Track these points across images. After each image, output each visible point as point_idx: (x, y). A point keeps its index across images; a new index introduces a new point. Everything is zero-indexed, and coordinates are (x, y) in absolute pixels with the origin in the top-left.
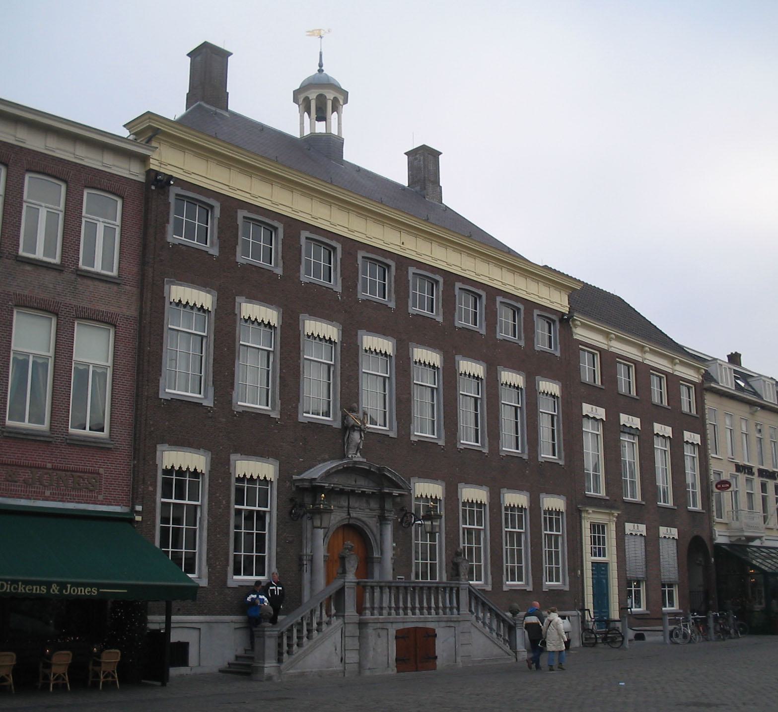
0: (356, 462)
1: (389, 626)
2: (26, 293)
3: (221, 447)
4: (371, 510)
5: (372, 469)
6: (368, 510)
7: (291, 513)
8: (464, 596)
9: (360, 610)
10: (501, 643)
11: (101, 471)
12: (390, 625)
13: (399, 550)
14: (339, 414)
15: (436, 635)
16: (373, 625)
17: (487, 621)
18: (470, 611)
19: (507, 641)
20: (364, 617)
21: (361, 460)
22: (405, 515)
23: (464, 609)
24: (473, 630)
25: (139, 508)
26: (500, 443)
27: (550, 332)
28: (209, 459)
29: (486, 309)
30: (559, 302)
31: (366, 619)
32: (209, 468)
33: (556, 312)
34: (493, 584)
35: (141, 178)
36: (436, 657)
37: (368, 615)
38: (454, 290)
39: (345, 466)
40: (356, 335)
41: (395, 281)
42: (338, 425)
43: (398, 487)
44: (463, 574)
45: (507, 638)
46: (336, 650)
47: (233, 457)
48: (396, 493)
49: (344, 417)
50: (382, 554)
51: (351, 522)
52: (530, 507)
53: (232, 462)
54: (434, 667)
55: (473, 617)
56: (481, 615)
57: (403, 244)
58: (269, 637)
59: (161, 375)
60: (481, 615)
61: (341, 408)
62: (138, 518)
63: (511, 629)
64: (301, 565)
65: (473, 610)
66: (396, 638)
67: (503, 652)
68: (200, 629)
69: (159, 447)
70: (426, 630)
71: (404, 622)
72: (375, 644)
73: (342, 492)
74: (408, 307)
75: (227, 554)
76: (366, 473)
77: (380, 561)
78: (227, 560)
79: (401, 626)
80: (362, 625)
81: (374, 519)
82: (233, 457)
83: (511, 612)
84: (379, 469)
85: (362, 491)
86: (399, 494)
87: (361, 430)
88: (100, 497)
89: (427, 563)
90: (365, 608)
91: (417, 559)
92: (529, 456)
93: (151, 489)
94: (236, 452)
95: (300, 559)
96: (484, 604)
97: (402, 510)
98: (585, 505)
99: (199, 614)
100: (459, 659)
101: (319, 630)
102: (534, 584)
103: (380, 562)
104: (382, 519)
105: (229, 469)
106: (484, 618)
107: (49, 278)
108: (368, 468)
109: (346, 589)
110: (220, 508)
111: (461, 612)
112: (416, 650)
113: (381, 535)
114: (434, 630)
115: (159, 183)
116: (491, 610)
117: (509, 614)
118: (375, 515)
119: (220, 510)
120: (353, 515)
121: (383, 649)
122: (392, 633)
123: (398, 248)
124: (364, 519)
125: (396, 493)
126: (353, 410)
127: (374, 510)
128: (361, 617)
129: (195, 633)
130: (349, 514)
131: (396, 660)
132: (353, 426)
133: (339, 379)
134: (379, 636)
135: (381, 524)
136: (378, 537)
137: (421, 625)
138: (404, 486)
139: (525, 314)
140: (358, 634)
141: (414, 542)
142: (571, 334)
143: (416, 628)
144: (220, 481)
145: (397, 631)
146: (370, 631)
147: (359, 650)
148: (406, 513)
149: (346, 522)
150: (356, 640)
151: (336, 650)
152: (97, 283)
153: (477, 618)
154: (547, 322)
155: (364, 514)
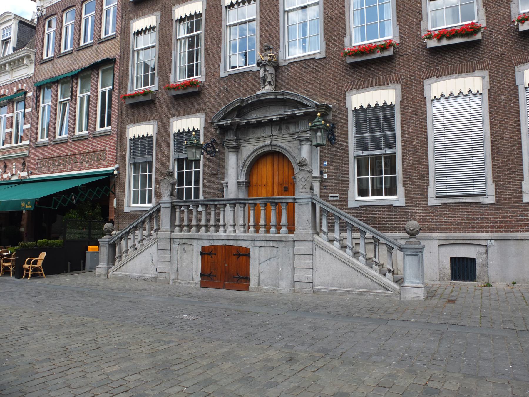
0: (258, 96)
4: (290, 134)
5: (278, 97)
6: (287, 136)
11: (107, 148)
12: (195, 241)
13: (332, 167)
15: (248, 255)
16: (178, 240)
32: (156, 132)
39: (250, 101)
48: (299, 112)
53: (170, 124)
66: (201, 254)
67: (376, 285)
70: (238, 248)
71: (210, 239)
79: (207, 243)
85: (269, 120)
86: (304, 112)
89: (382, 177)
93: (124, 153)
108: (274, 97)
112: (226, 268)
114: (247, 250)
122: (198, 247)
125: (299, 112)
131: (201, 275)
134: (184, 250)
137: (231, 243)
138: (308, 104)
145: (203, 248)
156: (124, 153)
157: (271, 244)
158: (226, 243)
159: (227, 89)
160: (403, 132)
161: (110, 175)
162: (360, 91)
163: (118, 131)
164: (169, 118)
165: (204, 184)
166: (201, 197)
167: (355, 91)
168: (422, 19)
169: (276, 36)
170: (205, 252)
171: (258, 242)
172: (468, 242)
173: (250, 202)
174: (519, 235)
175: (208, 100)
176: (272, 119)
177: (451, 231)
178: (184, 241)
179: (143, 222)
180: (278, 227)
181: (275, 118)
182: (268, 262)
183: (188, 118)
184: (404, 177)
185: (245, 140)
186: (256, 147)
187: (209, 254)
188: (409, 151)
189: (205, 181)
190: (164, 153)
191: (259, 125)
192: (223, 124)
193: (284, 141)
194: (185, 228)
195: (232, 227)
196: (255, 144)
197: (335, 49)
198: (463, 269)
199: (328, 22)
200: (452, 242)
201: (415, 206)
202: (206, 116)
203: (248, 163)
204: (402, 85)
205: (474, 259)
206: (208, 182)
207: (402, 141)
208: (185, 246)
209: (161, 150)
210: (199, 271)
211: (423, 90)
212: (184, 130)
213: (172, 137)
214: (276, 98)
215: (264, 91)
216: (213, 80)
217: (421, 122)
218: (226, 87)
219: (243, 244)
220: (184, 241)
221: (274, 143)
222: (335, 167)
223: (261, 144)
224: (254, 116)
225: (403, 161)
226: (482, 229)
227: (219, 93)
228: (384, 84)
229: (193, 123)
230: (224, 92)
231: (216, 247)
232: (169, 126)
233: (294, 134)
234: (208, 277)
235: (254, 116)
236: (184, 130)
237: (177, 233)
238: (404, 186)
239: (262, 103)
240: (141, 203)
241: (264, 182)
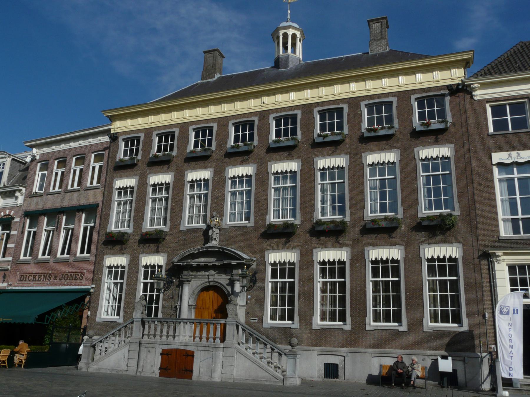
2: (67, 204)
11: (85, 271)
28: (129, 259)
32: (128, 263)
34: (353, 324)
36: (192, 371)
40: (225, 171)
48: (234, 262)
51: (211, 284)
53: (140, 258)
54: (190, 377)
57: (264, 103)
62: (92, 290)
66: (161, 354)
79: (166, 347)
88: (84, 283)
92: (461, 211)
93: (100, 276)
98: (500, 248)
107: (75, 194)
114: (193, 352)
125: (234, 262)
131: (160, 369)
134: (149, 351)
137: (182, 348)
145: (163, 350)
146: (142, 348)
149: (208, 284)
152: (91, 191)
156: (100, 276)
158: (180, 347)
159: (185, 239)
160: (300, 280)
161: (87, 292)
162: (274, 251)
163: (95, 260)
164: (139, 254)
165: (163, 305)
166: (160, 315)
167: (271, 251)
168: (314, 211)
169: (221, 208)
170: (164, 353)
172: (334, 353)
173: (197, 321)
174: (363, 350)
177: (325, 346)
178: (149, 345)
179: (119, 330)
184: (299, 310)
185: (195, 276)
186: (203, 282)
187: (167, 354)
188: (302, 293)
190: (133, 279)
195: (184, 337)
197: (260, 222)
198: (331, 371)
199: (257, 203)
200: (325, 353)
201: (305, 329)
202: (168, 256)
203: (196, 292)
205: (337, 365)
206: (165, 304)
207: (299, 286)
208: (150, 348)
209: (131, 277)
210: (159, 366)
214: (218, 251)
215: (211, 245)
217: (311, 275)
218: (184, 237)
221: (216, 280)
222: (256, 300)
223: (207, 280)
224: (202, 260)
225: (299, 299)
226: (342, 346)
227: (179, 241)
229: (158, 260)
230: (182, 240)
232: (139, 260)
238: (299, 315)
241: (207, 306)
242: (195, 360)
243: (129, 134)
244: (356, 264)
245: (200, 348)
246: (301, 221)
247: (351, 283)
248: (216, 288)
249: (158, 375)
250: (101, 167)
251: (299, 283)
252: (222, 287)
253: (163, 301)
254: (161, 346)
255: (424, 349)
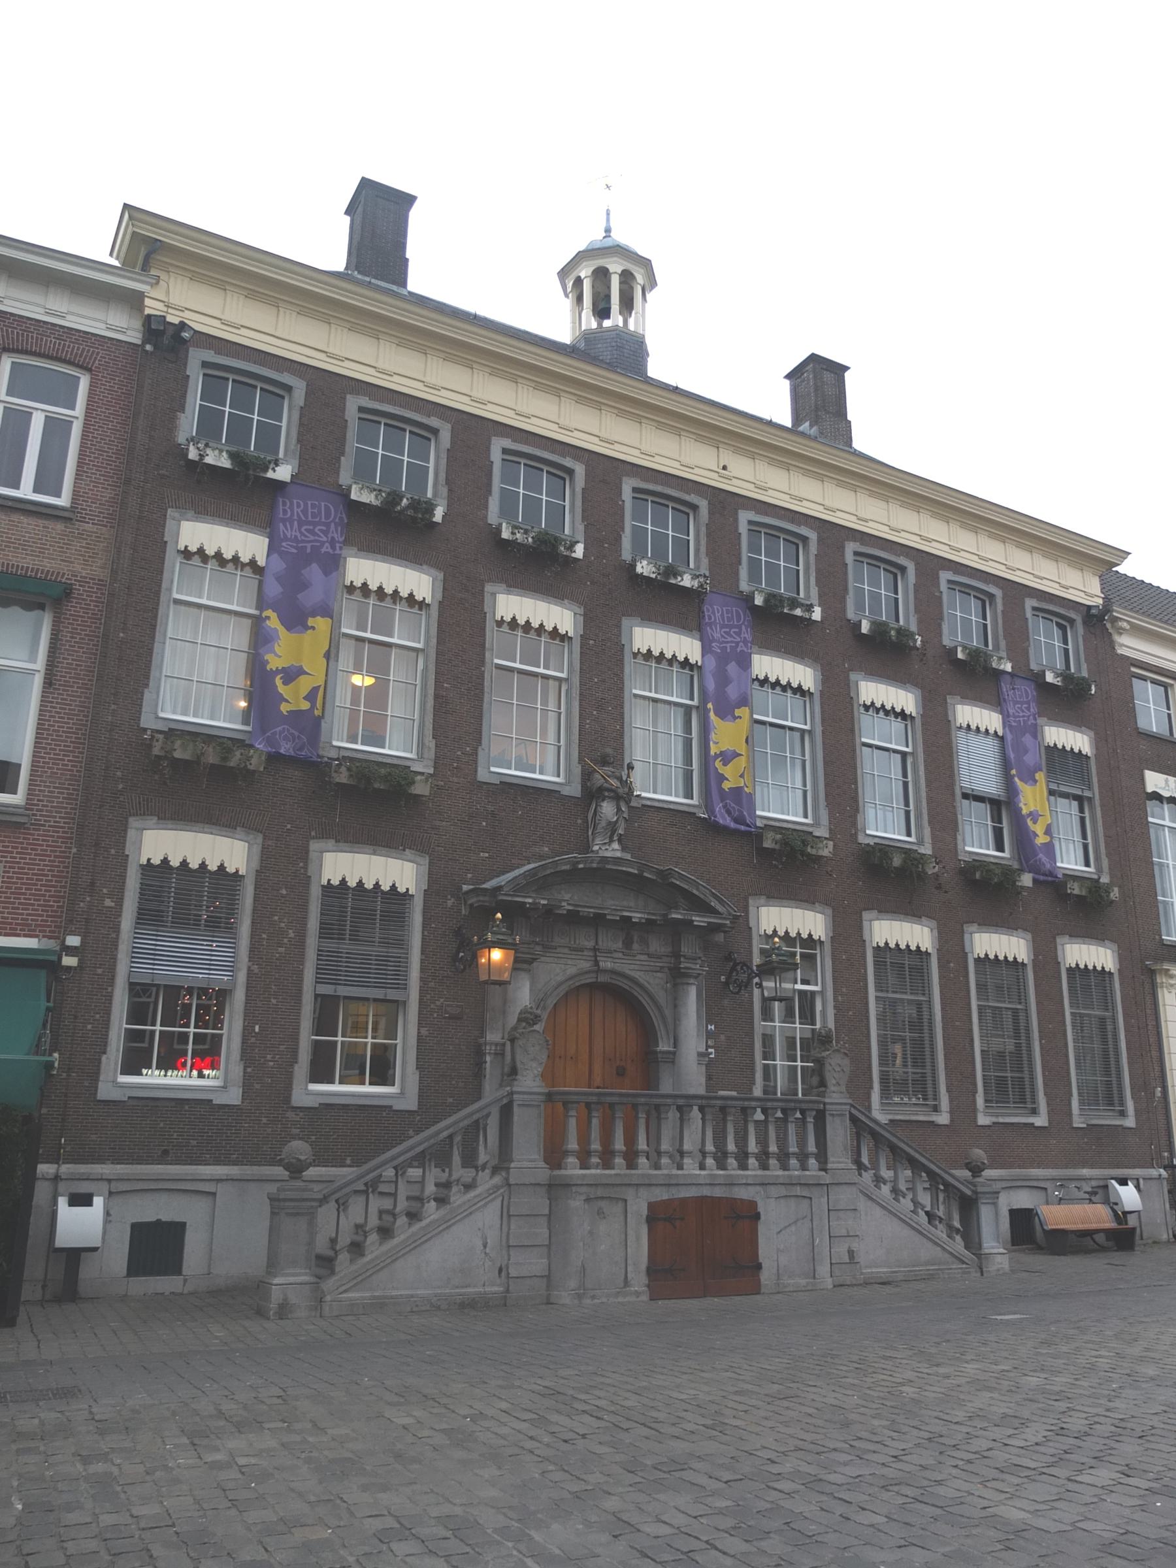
0: (604, 859)
1: (629, 1194)
3: (289, 826)
5: (646, 874)
7: (455, 958)
8: (838, 1133)
9: (554, 1155)
10: (941, 1233)
13: (722, 1037)
14: (577, 770)
15: (757, 1216)
16: (584, 1189)
17: (902, 1186)
18: (860, 1166)
19: (958, 1231)
20: (563, 1172)
21: (618, 854)
22: (733, 969)
23: (840, 1159)
24: (862, 1204)
25: (73, 941)
26: (959, 837)
27: (1065, 642)
28: (257, 849)
29: (916, 591)
30: (1085, 589)
31: (571, 1176)
33: (1075, 605)
34: (951, 1112)
35: (134, 336)
36: (759, 1267)
37: (572, 1170)
38: (843, 555)
39: (581, 866)
41: (708, 535)
42: (575, 790)
43: (703, 907)
44: (834, 1082)
45: (957, 1224)
46: (485, 1246)
47: (314, 846)
48: (699, 920)
49: (587, 775)
50: (675, 1046)
51: (602, 978)
52: (1035, 962)
53: (313, 855)
54: (756, 1289)
55: (867, 1176)
56: (887, 1174)
58: (288, 1214)
59: (147, 685)
60: (887, 1174)
61: (581, 760)
63: (968, 1205)
64: (480, 1064)
65: (865, 1160)
66: (651, 1220)
67: (947, 1255)
68: (214, 1194)
69: (134, 822)
70: (732, 1203)
71: (669, 1185)
72: (591, 1233)
73: (574, 919)
74: (738, 580)
75: (295, 1038)
76: (635, 884)
77: (672, 1058)
78: (295, 1052)
79: (662, 1195)
80: (556, 1189)
81: (659, 974)
82: (314, 846)
83: (968, 1166)
84: (660, 873)
85: (622, 917)
86: (709, 923)
87: (617, 798)
90: (566, 1153)
91: (768, 1054)
94: (324, 835)
95: (479, 1053)
96: (893, 1149)
97: (729, 958)
98: (1163, 959)
99: (217, 1162)
100: (824, 1270)
101: (441, 1201)
102: (1051, 1112)
103: (673, 1062)
104: (677, 977)
105: (306, 868)
106: (895, 1180)
109: (516, 1109)
110: (280, 945)
111: (830, 1166)
112: (706, 1252)
113: (675, 1006)
114: (753, 1204)
115: (167, 340)
116: (914, 1164)
117: (967, 1174)
118: (662, 967)
119: (282, 950)
120: (606, 964)
121: (616, 1245)
122: (639, 1206)
123: (715, 476)
124: (637, 975)
125: (699, 920)
126: (604, 761)
127: (659, 957)
128: (557, 1172)
129: (202, 1204)
130: (596, 963)
131: (650, 1271)
132: (601, 789)
133: (576, 704)
134: (600, 1213)
135: (675, 985)
136: (668, 1012)
137: (718, 1192)
139: (1004, 604)
140: (546, 1212)
141: (760, 1025)
142: (1112, 645)
143: (703, 1199)
144: (284, 892)
145: (651, 1206)
147: (549, 1246)
148: (736, 964)
150: (543, 1221)
151: (485, 1246)
153: (879, 1180)
154: (1058, 624)
155: (638, 968)
157: (798, 1191)
158: (706, 1191)
170: (657, 1216)
171: (772, 1187)
175: (438, 823)
176: (631, 918)
178: (600, 1192)
180: (803, 1157)
181: (636, 916)
182: (793, 1228)
183: (374, 853)
185: (547, 948)
186: (572, 971)
189: (424, 1031)
191: (598, 921)
192: (525, 903)
193: (636, 967)
194: (595, 1160)
196: (570, 962)
204: (834, 910)
208: (602, 1204)
211: (861, 928)
212: (377, 885)
213: (315, 893)
214: (639, 877)
216: (455, 780)
218: (490, 808)
219: (743, 1194)
220: (600, 1192)
221: (618, 967)
228: (806, 901)
231: (684, 1201)
233: (659, 957)
234: (666, 1276)
235: (567, 899)
236: (377, 885)
237: (572, 1170)
239: (603, 875)
240: (371, 1084)
242: (761, 1228)
243: (236, 356)
244: (948, 962)
245: (774, 1191)
246: (830, 830)
247: (942, 1009)
248: (617, 994)
249: (645, 1298)
250: (56, 430)
251: (835, 999)
252: (637, 992)
253: (420, 1025)
254: (643, 1192)
255: (1075, 1167)
